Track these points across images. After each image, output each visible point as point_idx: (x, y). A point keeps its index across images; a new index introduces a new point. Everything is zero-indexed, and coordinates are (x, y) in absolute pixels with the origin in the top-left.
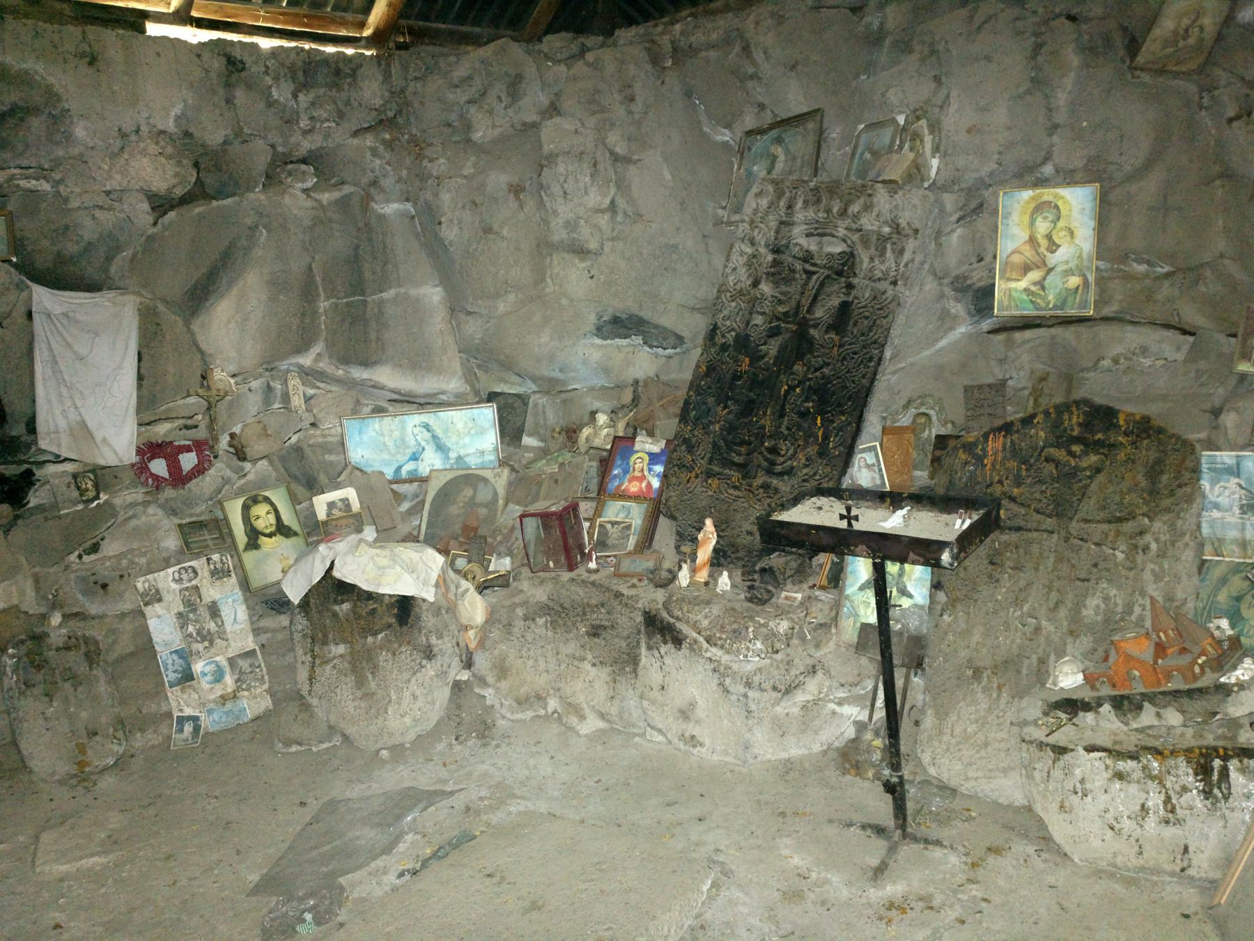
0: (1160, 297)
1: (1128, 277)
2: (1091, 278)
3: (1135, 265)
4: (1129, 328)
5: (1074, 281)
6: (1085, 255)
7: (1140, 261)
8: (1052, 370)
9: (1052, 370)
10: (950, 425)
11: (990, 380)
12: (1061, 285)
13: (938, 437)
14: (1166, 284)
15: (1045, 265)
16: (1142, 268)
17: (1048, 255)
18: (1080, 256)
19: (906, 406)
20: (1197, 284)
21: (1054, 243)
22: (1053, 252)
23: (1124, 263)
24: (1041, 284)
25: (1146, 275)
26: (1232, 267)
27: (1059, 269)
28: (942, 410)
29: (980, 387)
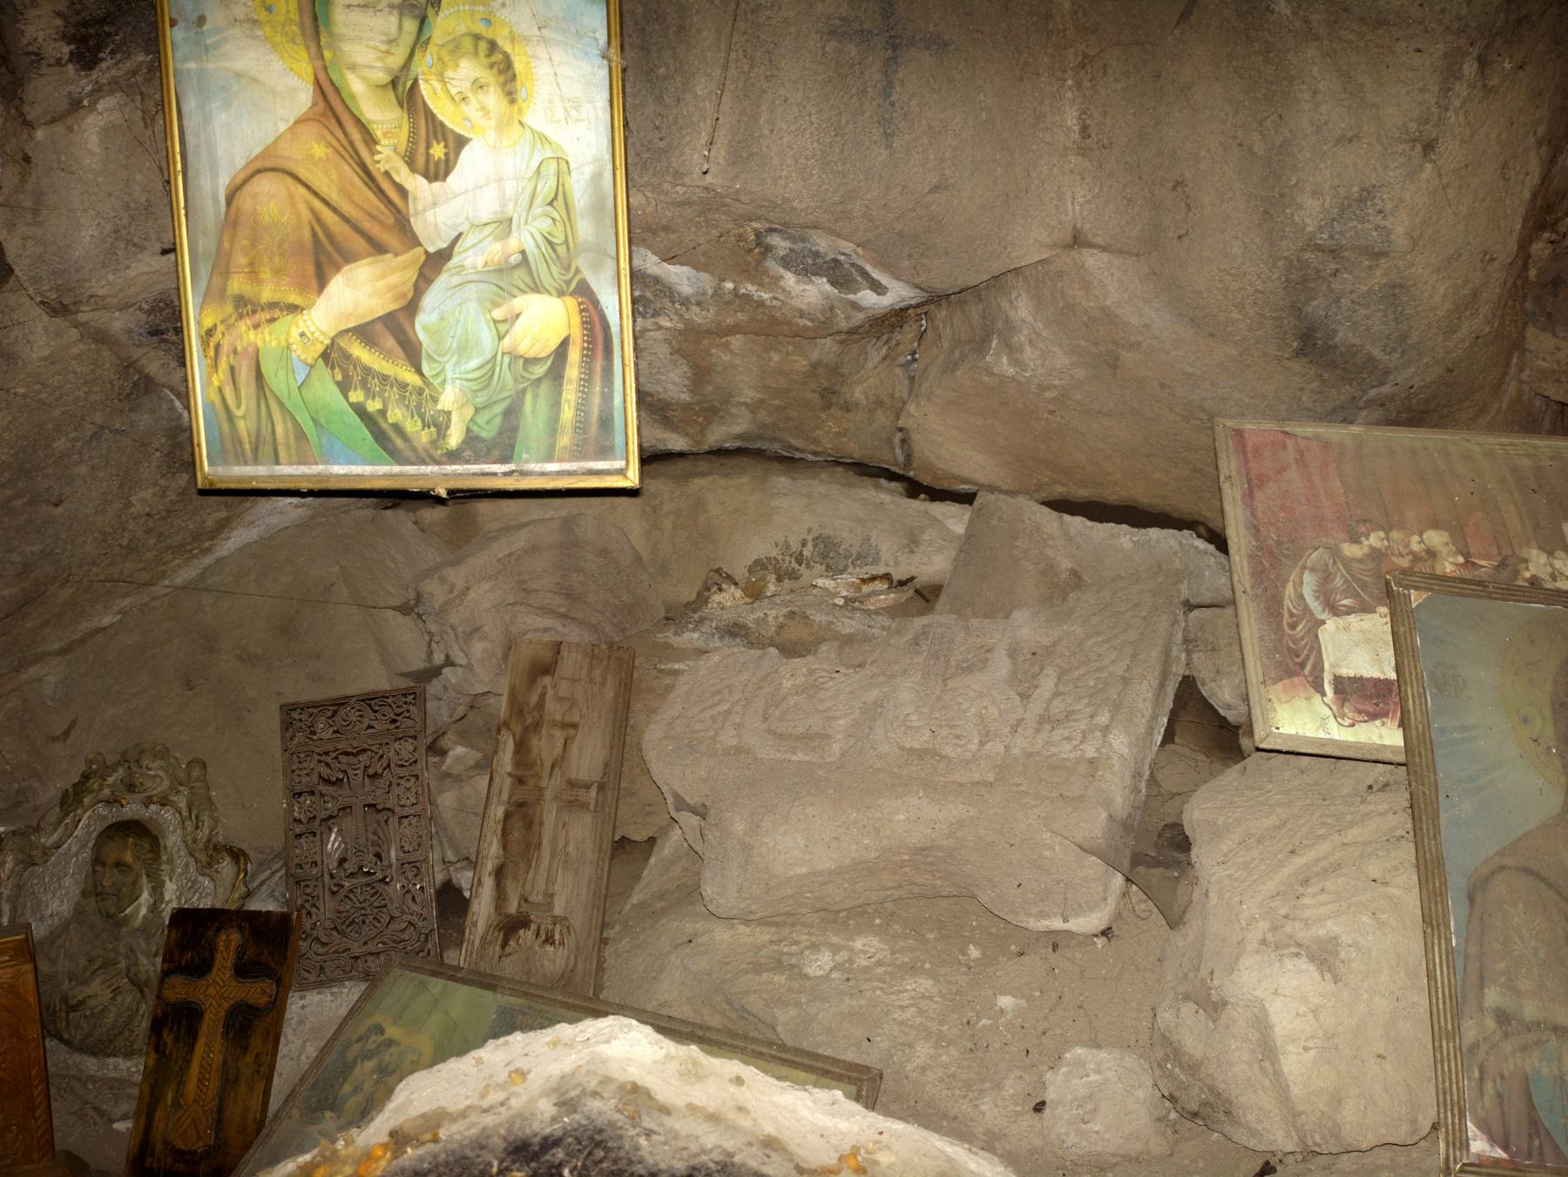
0: (858, 394)
1: (772, 327)
2: (614, 303)
3: (790, 280)
4: (782, 481)
5: (544, 320)
6: (579, 193)
7: (808, 265)
8: (574, 634)
9: (574, 634)
10: (226, 867)
11: (376, 680)
12: (487, 336)
13: (183, 917)
14: (875, 353)
15: (413, 241)
16: (810, 293)
17: (416, 184)
18: (559, 198)
19: (71, 800)
20: (981, 346)
21: (437, 129)
22: (437, 172)
23: (755, 272)
24: (395, 329)
25: (823, 326)
26: (1109, 280)
27: (475, 256)
28: (193, 815)
29: (340, 703)
